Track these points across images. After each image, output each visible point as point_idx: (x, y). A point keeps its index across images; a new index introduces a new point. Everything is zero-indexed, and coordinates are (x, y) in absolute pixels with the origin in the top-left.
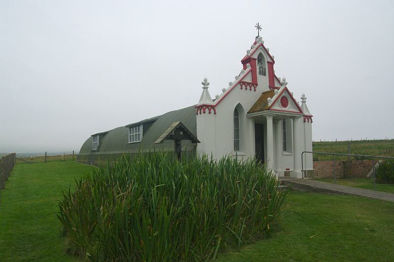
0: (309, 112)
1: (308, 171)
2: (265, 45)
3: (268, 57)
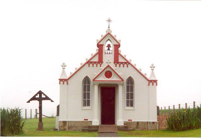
0: (154, 76)
1: (150, 122)
2: (113, 34)
3: (114, 41)
